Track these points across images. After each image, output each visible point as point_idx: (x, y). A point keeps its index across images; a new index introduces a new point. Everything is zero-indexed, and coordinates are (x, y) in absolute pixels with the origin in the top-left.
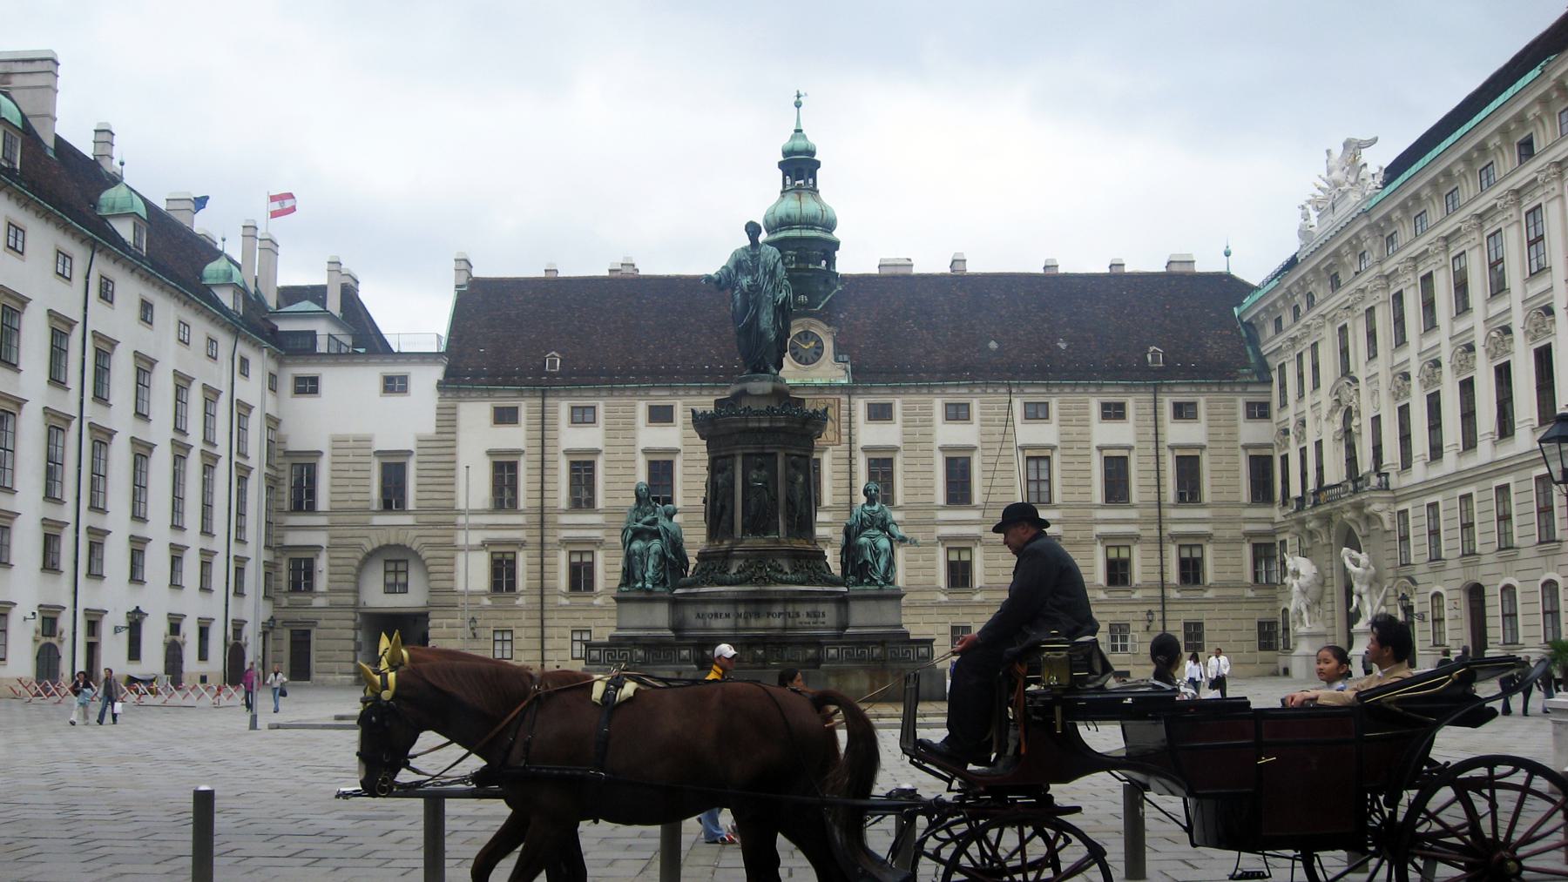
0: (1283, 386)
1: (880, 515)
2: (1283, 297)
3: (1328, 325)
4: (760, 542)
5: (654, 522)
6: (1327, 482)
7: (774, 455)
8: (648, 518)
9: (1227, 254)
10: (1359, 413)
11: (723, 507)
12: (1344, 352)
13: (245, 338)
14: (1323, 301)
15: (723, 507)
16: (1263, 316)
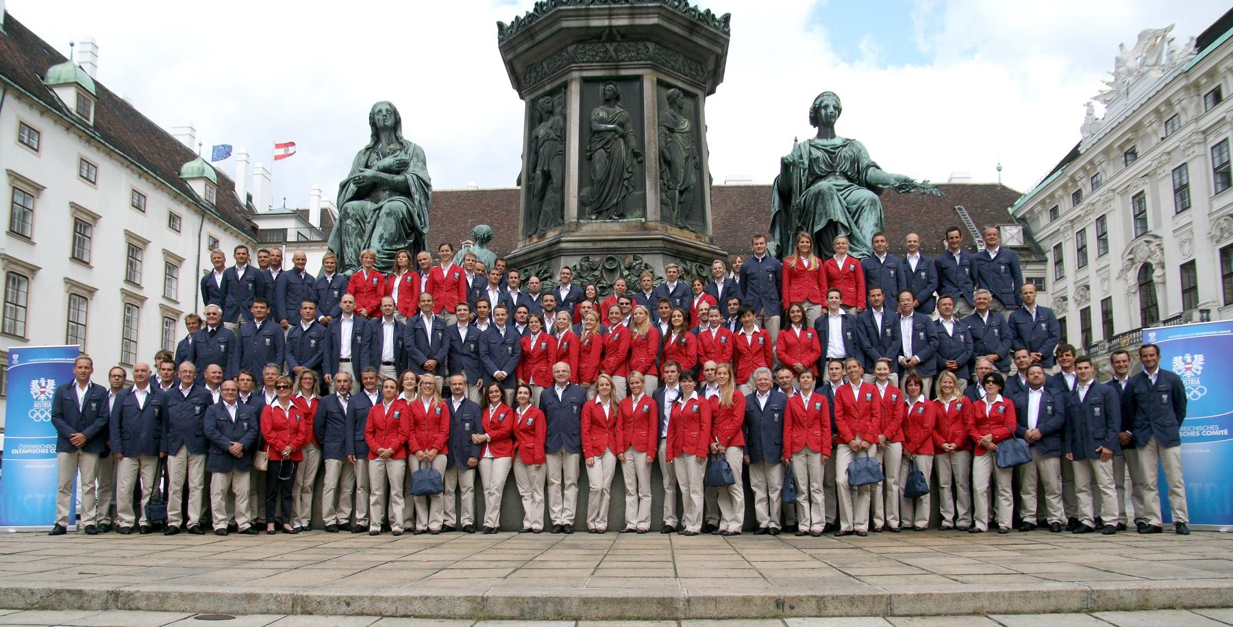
0: (1059, 262)
1: (846, 152)
2: (1064, 187)
3: (1118, 199)
4: (610, 228)
5: (402, 167)
6: (1116, 332)
7: (639, 78)
8: (388, 161)
9: (999, 170)
10: (1163, 267)
11: (547, 176)
12: (1140, 217)
13: (214, 222)
14: (1112, 179)
15: (547, 176)
16: (1039, 208)
